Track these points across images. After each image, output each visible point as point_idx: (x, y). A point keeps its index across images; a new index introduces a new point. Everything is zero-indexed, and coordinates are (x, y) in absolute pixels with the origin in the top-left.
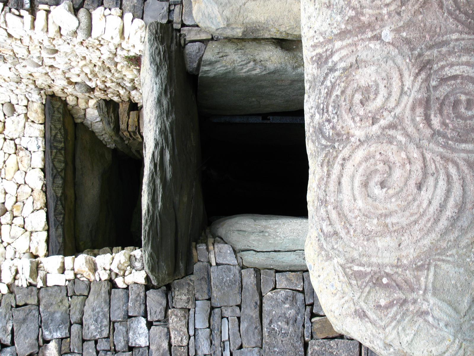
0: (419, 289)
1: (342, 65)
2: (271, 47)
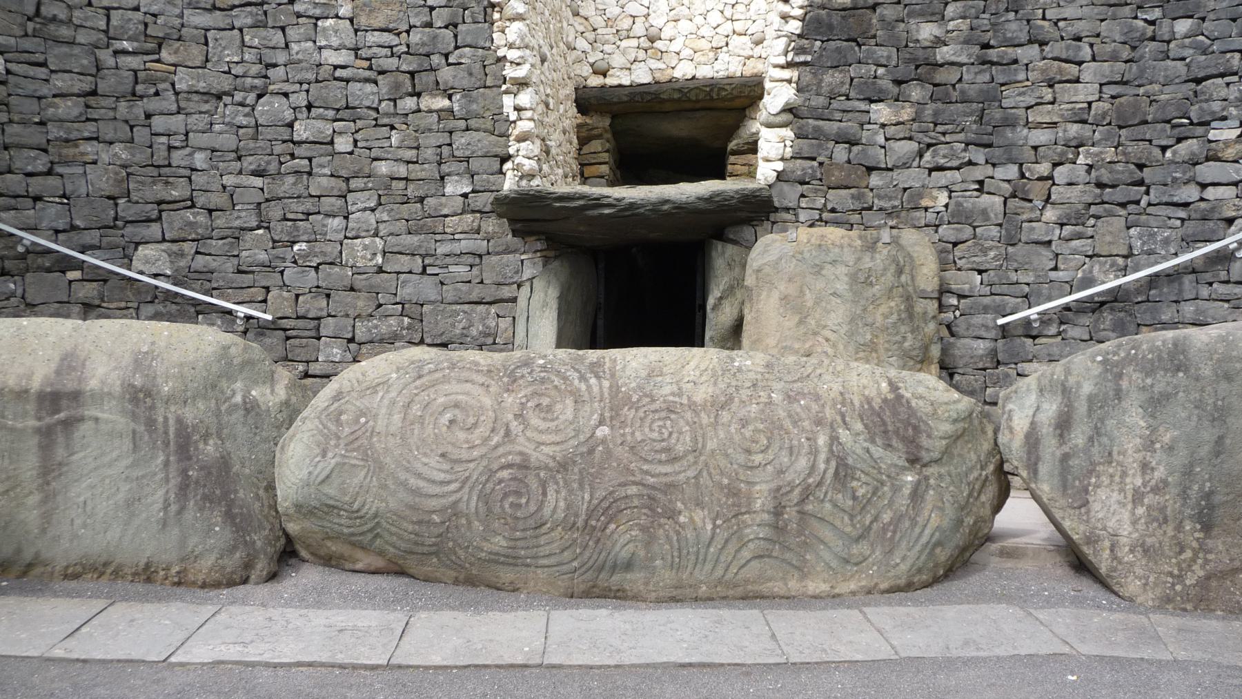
0: (347, 451)
1: (583, 387)
2: (735, 312)
